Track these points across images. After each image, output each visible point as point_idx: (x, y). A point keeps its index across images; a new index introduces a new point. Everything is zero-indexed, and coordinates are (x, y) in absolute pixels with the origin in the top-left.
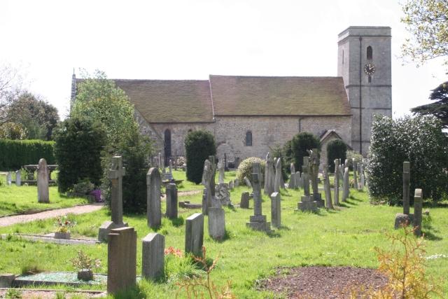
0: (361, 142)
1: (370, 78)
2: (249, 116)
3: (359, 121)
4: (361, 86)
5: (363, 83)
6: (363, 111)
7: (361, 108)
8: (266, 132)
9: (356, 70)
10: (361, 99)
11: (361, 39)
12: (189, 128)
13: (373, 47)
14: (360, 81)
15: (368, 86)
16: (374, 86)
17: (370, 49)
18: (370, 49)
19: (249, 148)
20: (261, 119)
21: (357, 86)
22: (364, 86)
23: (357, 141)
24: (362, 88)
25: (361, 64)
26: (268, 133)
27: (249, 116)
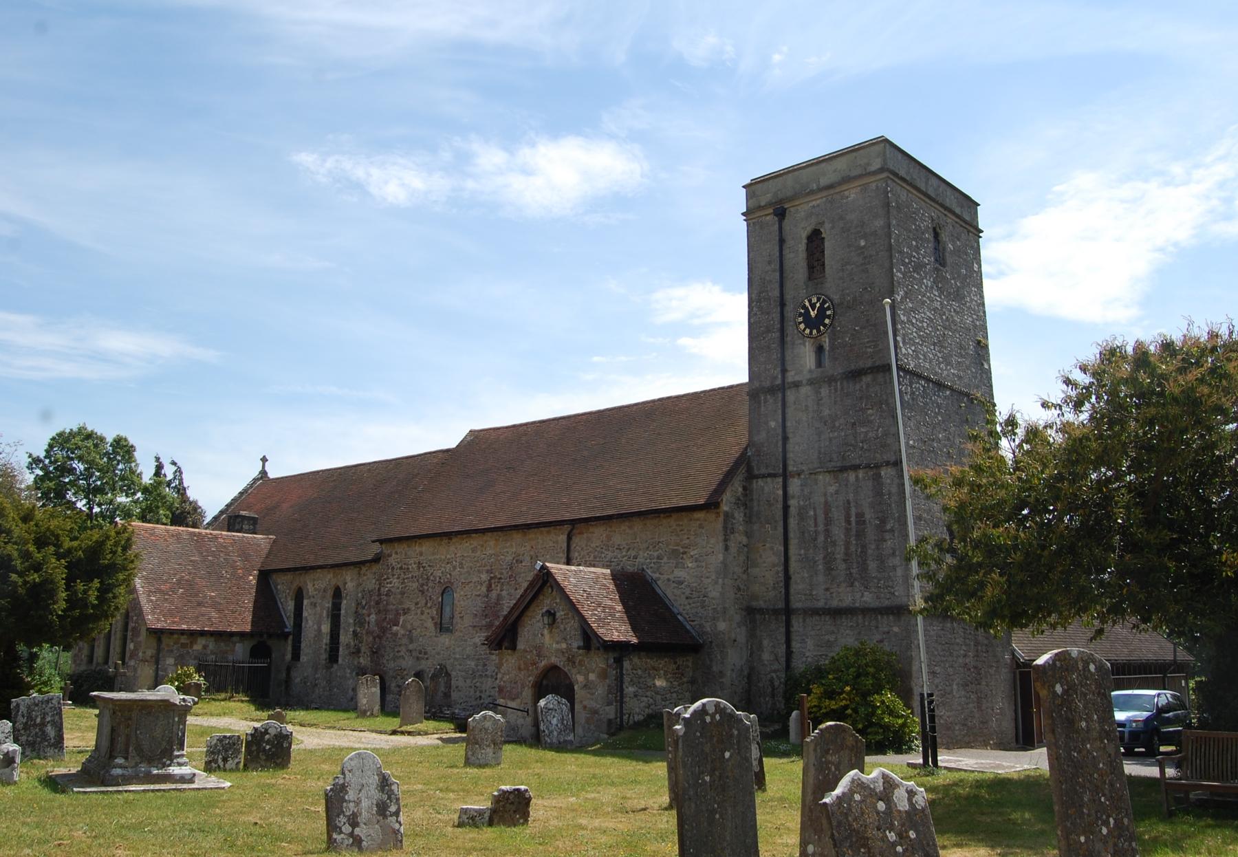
0: (788, 612)
1: (820, 350)
2: (449, 535)
3: (781, 529)
4: (783, 388)
5: (791, 377)
6: (795, 485)
7: (785, 475)
8: (484, 589)
9: (768, 331)
10: (785, 439)
11: (781, 214)
12: (334, 582)
13: (826, 232)
14: (784, 371)
15: (811, 382)
16: (831, 380)
17: (815, 238)
18: (815, 238)
19: (445, 640)
20: (475, 541)
21: (772, 390)
22: (797, 385)
23: (776, 612)
24: (791, 396)
25: (783, 304)
26: (489, 589)
27: (449, 535)
